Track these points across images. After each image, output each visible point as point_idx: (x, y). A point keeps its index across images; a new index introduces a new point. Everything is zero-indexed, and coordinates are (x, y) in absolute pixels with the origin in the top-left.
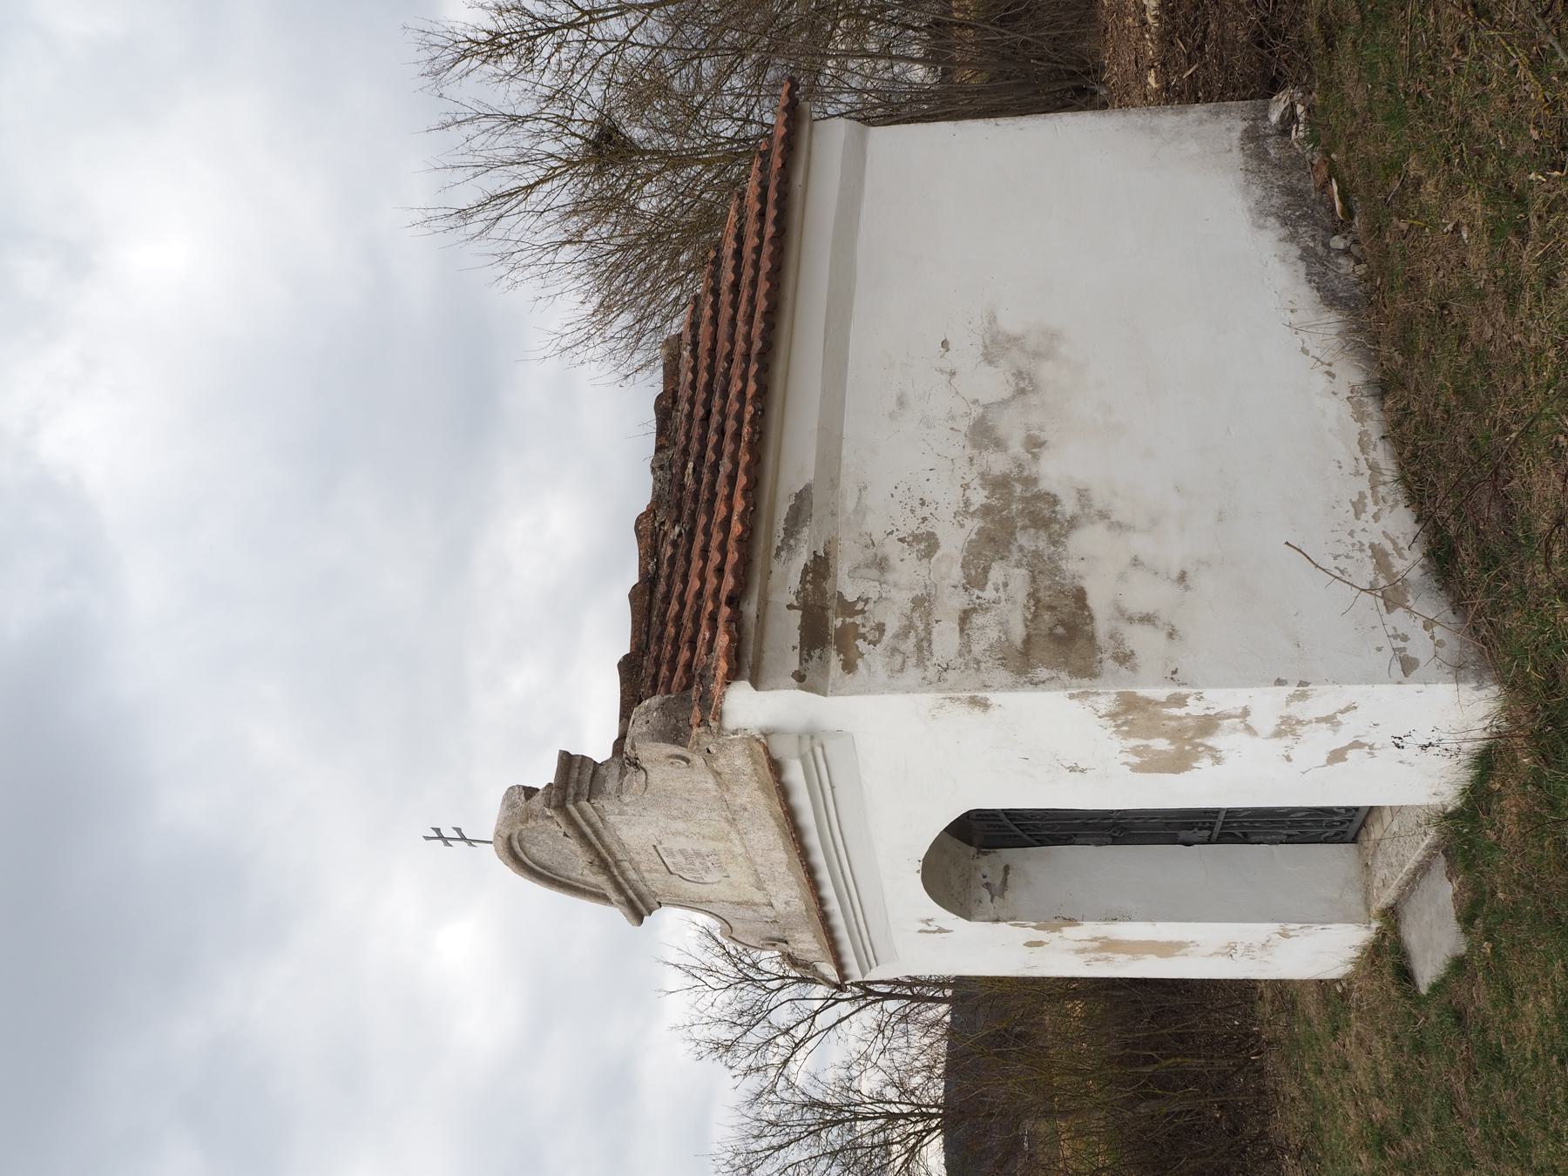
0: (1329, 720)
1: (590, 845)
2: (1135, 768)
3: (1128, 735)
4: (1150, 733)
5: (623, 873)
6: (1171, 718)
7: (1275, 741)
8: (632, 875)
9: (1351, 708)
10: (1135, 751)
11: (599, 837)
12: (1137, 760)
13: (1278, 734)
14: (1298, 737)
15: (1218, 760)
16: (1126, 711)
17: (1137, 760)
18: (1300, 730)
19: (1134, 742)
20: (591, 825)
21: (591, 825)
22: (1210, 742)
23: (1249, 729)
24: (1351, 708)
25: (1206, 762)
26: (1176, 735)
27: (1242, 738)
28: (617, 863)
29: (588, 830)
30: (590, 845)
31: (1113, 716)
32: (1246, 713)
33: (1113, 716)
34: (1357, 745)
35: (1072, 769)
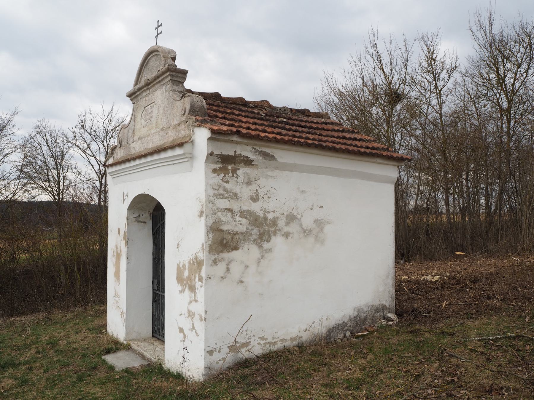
0: (193, 328)
1: (155, 80)
2: (178, 265)
3: (190, 263)
4: (190, 270)
5: (145, 91)
7: (187, 311)
8: (144, 94)
10: (184, 265)
12: (181, 266)
13: (189, 311)
14: (188, 318)
15: (181, 292)
16: (197, 262)
17: (181, 266)
18: (190, 318)
20: (162, 80)
21: (162, 80)
23: (191, 302)
25: (180, 288)
26: (189, 278)
27: (188, 300)
28: (148, 89)
29: (160, 79)
30: (155, 80)
31: (196, 258)
32: (196, 301)
33: (196, 258)
34: (185, 336)
35: (178, 244)
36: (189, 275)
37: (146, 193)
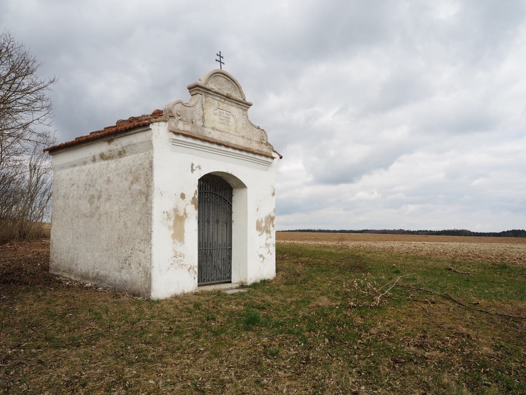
0: (269, 251)
1: (236, 101)
2: (258, 221)
3: (265, 219)
4: (266, 222)
5: (221, 98)
8: (217, 98)
10: (262, 221)
11: (237, 104)
12: (260, 220)
13: (266, 244)
15: (260, 235)
17: (260, 220)
18: (267, 248)
19: (264, 220)
22: (264, 233)
25: (259, 233)
26: (266, 227)
27: (266, 238)
29: (241, 104)
30: (236, 101)
31: (270, 216)
32: (271, 237)
33: (270, 216)
34: (264, 258)
36: (266, 225)
37: (230, 172)
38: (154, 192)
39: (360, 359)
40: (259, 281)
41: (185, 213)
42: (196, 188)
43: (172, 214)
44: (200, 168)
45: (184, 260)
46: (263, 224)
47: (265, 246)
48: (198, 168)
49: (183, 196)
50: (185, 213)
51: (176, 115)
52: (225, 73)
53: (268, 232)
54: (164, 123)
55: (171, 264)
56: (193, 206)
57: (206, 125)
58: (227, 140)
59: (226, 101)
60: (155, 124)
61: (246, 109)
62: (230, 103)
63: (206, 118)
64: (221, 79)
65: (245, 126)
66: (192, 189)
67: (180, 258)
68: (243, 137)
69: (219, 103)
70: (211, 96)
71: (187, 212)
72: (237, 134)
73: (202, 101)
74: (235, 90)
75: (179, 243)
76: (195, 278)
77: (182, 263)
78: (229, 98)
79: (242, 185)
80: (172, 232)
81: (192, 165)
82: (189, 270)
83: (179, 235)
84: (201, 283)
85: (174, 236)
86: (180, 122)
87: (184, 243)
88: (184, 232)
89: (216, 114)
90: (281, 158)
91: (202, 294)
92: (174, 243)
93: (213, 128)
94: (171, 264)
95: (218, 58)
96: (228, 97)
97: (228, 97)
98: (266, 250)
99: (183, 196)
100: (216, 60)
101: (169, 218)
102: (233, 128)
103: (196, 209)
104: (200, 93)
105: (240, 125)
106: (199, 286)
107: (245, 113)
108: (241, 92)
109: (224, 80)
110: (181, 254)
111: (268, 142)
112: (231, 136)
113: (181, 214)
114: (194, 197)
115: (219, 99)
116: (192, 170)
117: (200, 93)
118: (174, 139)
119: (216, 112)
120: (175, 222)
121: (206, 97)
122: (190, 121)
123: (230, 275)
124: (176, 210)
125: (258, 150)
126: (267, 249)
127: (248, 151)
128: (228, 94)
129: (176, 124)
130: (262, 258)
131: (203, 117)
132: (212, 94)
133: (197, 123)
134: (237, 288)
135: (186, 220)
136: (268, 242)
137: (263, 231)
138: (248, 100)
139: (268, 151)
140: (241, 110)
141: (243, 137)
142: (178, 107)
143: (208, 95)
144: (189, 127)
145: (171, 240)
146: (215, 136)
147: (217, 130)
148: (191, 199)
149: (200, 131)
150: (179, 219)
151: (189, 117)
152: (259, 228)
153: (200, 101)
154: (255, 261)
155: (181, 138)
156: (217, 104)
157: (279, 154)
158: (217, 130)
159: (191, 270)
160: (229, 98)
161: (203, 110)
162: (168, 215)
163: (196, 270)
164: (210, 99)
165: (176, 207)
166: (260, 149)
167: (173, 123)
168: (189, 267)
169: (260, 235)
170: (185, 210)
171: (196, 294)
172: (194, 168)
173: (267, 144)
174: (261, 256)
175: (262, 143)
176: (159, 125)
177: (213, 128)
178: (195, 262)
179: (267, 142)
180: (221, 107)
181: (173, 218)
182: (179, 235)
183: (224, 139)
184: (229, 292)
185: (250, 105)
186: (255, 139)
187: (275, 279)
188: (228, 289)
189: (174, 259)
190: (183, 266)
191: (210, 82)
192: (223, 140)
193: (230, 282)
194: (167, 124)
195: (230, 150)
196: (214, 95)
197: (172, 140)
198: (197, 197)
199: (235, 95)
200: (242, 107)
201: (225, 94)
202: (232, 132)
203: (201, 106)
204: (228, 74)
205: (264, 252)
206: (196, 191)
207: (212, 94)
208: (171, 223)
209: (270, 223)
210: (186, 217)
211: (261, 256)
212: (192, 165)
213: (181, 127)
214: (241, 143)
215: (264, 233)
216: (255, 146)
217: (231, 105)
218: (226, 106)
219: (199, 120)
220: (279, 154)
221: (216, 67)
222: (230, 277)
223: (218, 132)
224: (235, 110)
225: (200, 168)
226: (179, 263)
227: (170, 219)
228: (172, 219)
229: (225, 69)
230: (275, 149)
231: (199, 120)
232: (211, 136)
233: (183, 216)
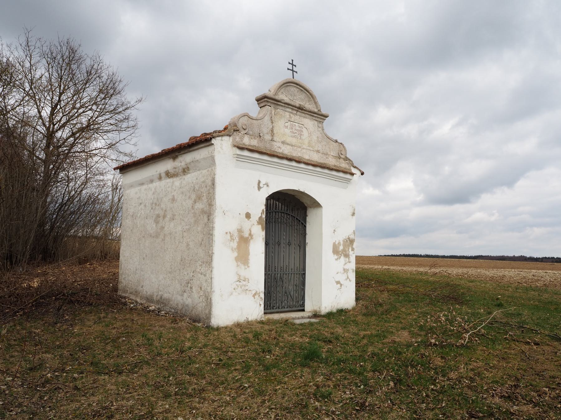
0: (348, 278)
2: (334, 244)
3: (344, 241)
4: (344, 245)
5: (292, 109)
6: (349, 249)
7: (342, 269)
8: (288, 110)
9: (350, 281)
10: (339, 243)
11: (310, 115)
12: (337, 243)
13: (344, 269)
14: (344, 273)
15: (336, 259)
16: (350, 241)
17: (337, 243)
19: (342, 243)
20: (316, 117)
21: (316, 117)
22: (342, 257)
23: (346, 263)
24: (350, 281)
25: (336, 257)
26: (344, 250)
27: (344, 263)
28: (297, 111)
29: (315, 115)
30: (310, 112)
31: (349, 238)
32: (349, 262)
33: (349, 238)
34: (341, 285)
35: (334, 230)
36: (344, 248)
37: (302, 190)
38: (216, 211)
39: (427, 409)
40: (335, 311)
41: (250, 234)
42: (264, 207)
43: (236, 234)
44: (268, 186)
45: (249, 284)
46: (341, 248)
47: (342, 272)
48: (265, 186)
49: (248, 216)
50: (250, 234)
51: (241, 129)
52: (298, 82)
53: (347, 256)
54: (228, 137)
55: (234, 289)
56: (260, 226)
57: (275, 139)
58: (299, 155)
59: (298, 113)
60: (218, 138)
61: (321, 120)
62: (303, 115)
63: (275, 132)
64: (294, 89)
65: (320, 140)
66: (259, 209)
67: (244, 283)
68: (318, 151)
69: (290, 115)
70: (281, 108)
71: (252, 233)
72: (311, 149)
73: (271, 113)
74: (309, 101)
75: (243, 267)
76: (260, 305)
77: (247, 288)
78: (302, 109)
79: (316, 205)
80: (236, 254)
81: (259, 182)
82: (254, 296)
83: (243, 258)
84: (269, 311)
85: (237, 259)
86: (246, 136)
87: (248, 267)
88: (249, 254)
89: (287, 127)
90: (362, 174)
91: (269, 322)
92: (238, 266)
93: (283, 143)
94: (234, 289)
95: (290, 67)
96: (300, 109)
97: (300, 109)
98: (345, 276)
99: (248, 216)
100: (288, 69)
101: (232, 239)
102: (306, 142)
103: (263, 230)
104: (269, 104)
105: (315, 138)
106: (265, 313)
107: (320, 125)
108: (316, 103)
109: (296, 90)
110: (245, 279)
111: (348, 156)
112: (304, 151)
113: (246, 235)
114: (261, 217)
115: (290, 110)
116: (259, 188)
117: (269, 104)
118: (238, 155)
119: (286, 124)
120: (239, 243)
121: (275, 109)
122: (257, 135)
123: (304, 303)
124: (240, 231)
125: (335, 166)
126: (345, 276)
127: (323, 166)
128: (300, 105)
129: (242, 138)
130: (339, 285)
131: (272, 131)
132: (282, 106)
133: (265, 137)
134: (309, 317)
135: (251, 241)
136: (346, 267)
137: (341, 255)
138: (324, 112)
139: (347, 166)
140: (316, 123)
141: (318, 151)
142: (244, 120)
143: (278, 107)
144: (256, 141)
145: (235, 264)
146: (286, 150)
147: (288, 144)
148: (257, 219)
149: (268, 146)
150: (244, 240)
151: (256, 131)
152: (336, 251)
153: (268, 113)
154: (331, 288)
155: (246, 153)
156: (288, 116)
157: (360, 170)
158: (288, 144)
159: (257, 296)
160: (302, 109)
161: (272, 122)
162: (231, 236)
163: (262, 296)
164: (280, 110)
165: (240, 228)
166: (337, 164)
167: (237, 137)
168: (254, 292)
169: (336, 259)
170: (250, 231)
171: (261, 322)
172: (261, 185)
173: (346, 159)
174: (338, 282)
175: (340, 158)
176: (222, 140)
177: (283, 143)
178: (261, 287)
179: (346, 157)
180: (292, 120)
181: (237, 239)
182: (243, 258)
183: (295, 153)
184: (298, 322)
185: (327, 117)
186: (332, 154)
187: (354, 309)
188: (299, 318)
189: (238, 283)
190: (247, 291)
191: (280, 93)
192: (294, 155)
193: (303, 310)
194: (231, 138)
195: (302, 166)
196: (284, 106)
197: (236, 156)
198: (264, 216)
199: (309, 106)
200: (317, 119)
201: (297, 105)
202: (304, 146)
203: (269, 118)
204: (301, 84)
205: (341, 278)
206: (263, 210)
207: (282, 106)
208: (235, 244)
209: (349, 246)
210: (252, 238)
211: (338, 282)
212: (259, 182)
213: (247, 141)
214: (316, 158)
215: (342, 257)
216: (332, 162)
217: (304, 117)
218: (298, 118)
219: (267, 133)
220: (360, 170)
221: (288, 76)
222: (303, 305)
223: (289, 147)
224: (309, 123)
225: (268, 186)
226: (243, 287)
227: (234, 240)
228: (235, 241)
229: (298, 78)
230: (355, 165)
231: (267, 133)
232: (280, 151)
233: (248, 238)
